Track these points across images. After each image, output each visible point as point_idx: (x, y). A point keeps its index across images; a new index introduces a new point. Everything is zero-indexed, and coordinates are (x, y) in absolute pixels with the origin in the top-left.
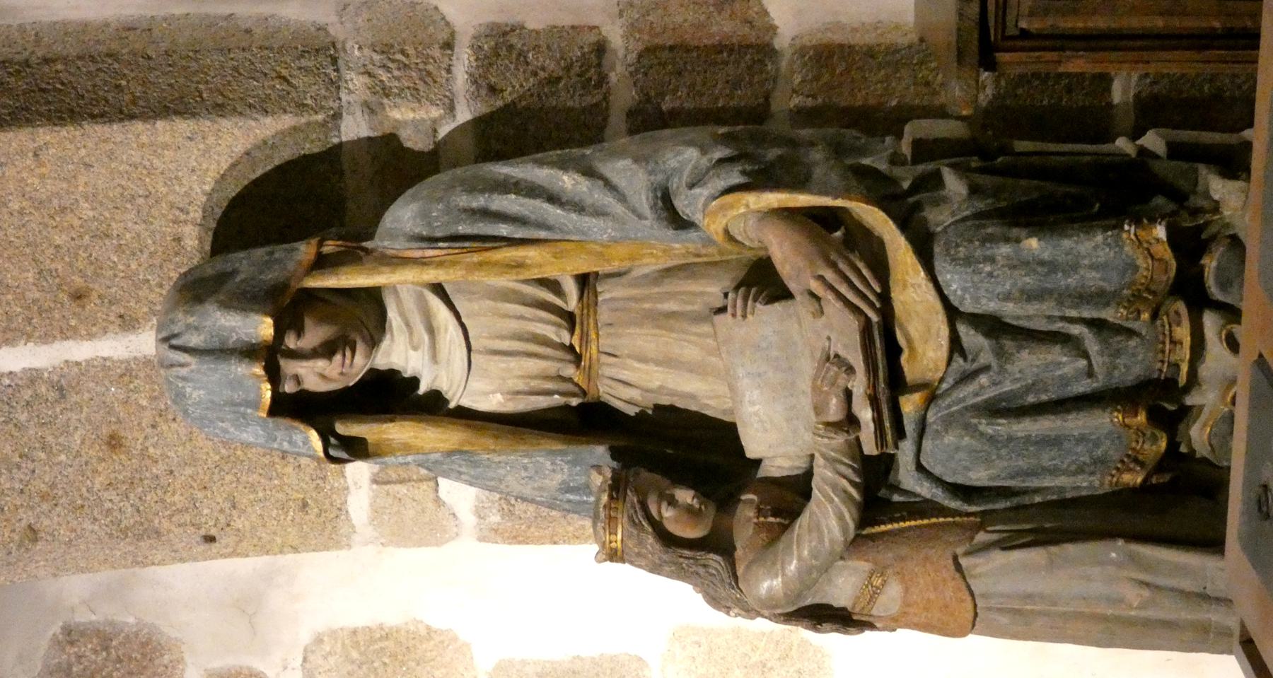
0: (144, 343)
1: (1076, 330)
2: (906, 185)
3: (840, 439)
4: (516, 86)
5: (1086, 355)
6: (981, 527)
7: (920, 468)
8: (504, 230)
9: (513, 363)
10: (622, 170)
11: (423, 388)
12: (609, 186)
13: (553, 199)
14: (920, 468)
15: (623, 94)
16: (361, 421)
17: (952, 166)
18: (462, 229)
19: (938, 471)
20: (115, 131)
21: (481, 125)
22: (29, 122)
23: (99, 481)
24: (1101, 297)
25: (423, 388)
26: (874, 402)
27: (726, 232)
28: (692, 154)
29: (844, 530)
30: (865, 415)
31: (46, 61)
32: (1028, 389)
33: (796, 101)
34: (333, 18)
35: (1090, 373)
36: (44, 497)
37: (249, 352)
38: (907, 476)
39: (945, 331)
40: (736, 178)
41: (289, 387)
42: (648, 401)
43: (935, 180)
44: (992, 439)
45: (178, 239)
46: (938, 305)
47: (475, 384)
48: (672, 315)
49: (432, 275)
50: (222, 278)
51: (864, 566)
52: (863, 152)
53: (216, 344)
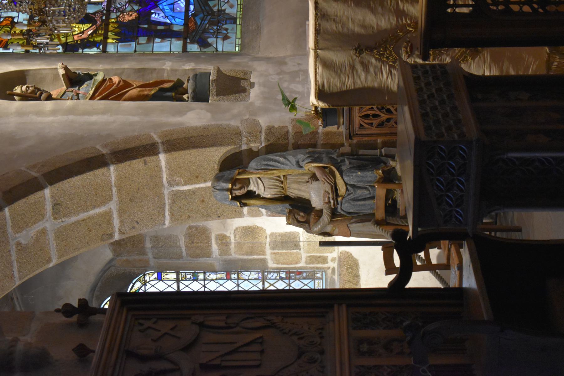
0: (209, 184)
1: (368, 187)
2: (339, 161)
3: (327, 205)
4: (273, 139)
5: (369, 191)
6: (351, 219)
7: (341, 209)
8: (270, 168)
9: (272, 190)
10: (290, 158)
11: (256, 193)
12: (288, 160)
13: (279, 162)
14: (341, 209)
15: (291, 140)
16: (246, 200)
17: (347, 158)
18: (263, 168)
19: (344, 210)
20: (203, 150)
21: (266, 146)
22: (189, 149)
23: (200, 208)
24: (371, 182)
25: (256, 193)
26: (333, 199)
27: (308, 169)
28: (302, 155)
29: (328, 220)
30: (332, 201)
31: (192, 137)
32: (360, 196)
33: (322, 142)
34: (240, 125)
35: (370, 194)
36: (191, 211)
37: (227, 190)
38: (339, 210)
39: (345, 187)
40: (310, 161)
41: (234, 195)
42: (296, 196)
43: (343, 161)
44: (353, 205)
45: (214, 167)
46: (344, 183)
47: (265, 193)
48: (300, 182)
49: (258, 176)
50: (222, 177)
51: (332, 226)
52: (332, 154)
53: (222, 188)
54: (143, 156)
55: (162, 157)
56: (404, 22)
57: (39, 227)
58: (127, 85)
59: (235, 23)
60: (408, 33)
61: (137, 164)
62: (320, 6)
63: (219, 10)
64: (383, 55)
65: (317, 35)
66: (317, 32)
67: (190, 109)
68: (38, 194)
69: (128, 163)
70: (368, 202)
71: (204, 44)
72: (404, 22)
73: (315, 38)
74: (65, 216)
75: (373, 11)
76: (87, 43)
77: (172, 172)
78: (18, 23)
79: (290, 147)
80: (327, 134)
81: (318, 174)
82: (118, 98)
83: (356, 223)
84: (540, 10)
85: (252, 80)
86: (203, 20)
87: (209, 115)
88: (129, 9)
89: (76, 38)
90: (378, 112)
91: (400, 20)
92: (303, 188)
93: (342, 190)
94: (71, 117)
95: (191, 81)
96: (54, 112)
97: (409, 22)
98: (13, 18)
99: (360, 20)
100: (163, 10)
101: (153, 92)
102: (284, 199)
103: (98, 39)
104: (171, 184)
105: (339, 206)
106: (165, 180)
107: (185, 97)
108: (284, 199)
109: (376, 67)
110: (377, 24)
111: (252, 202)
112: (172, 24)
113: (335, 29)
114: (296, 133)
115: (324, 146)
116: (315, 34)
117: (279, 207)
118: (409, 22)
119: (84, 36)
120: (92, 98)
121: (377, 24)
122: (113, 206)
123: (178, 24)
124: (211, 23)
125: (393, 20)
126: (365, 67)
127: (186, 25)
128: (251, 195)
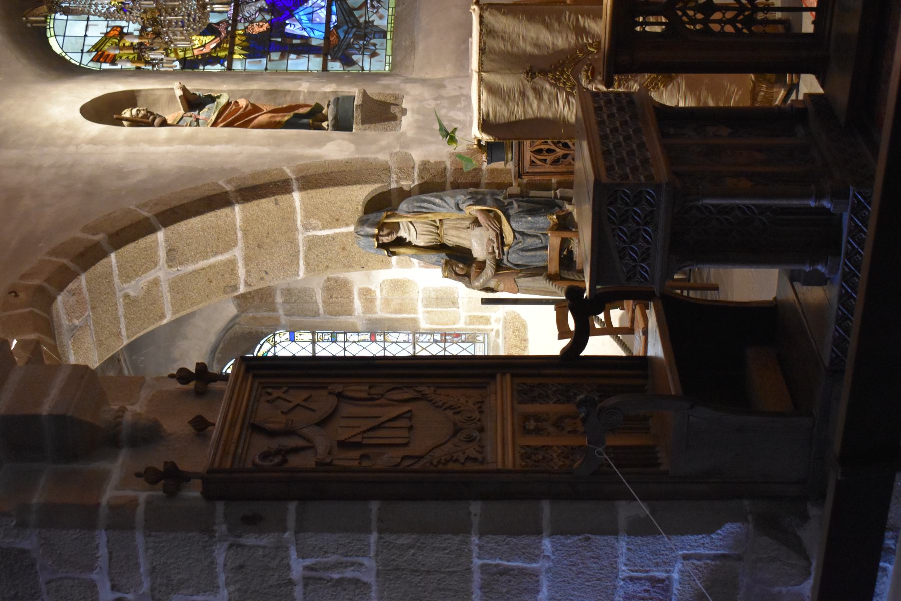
1: (539, 235)
2: (506, 204)
3: (491, 256)
4: (427, 177)
5: (541, 239)
6: (519, 273)
7: (508, 261)
8: (424, 210)
9: (426, 237)
10: (448, 199)
11: (407, 241)
12: (446, 202)
13: (434, 204)
14: (508, 261)
15: (450, 178)
17: (515, 200)
18: (416, 210)
19: (511, 262)
20: (345, 188)
21: (420, 185)
22: (328, 187)
23: (341, 257)
24: (543, 229)
25: (407, 241)
26: (498, 249)
27: (469, 213)
28: (462, 197)
29: (492, 274)
30: (496, 251)
31: (331, 173)
32: (530, 246)
33: (486, 181)
34: (389, 159)
35: (542, 243)
36: (330, 260)
37: (373, 236)
38: (505, 262)
39: (512, 235)
40: (471, 203)
41: (381, 242)
42: (455, 244)
43: (511, 204)
44: (522, 256)
45: (357, 208)
46: (511, 230)
47: (418, 240)
48: (459, 228)
49: (410, 220)
50: (368, 220)
51: (496, 280)
52: (498, 195)
53: (366, 234)
54: (274, 194)
55: (297, 196)
56: (585, 41)
57: (150, 276)
58: (256, 109)
59: (385, 37)
60: (589, 54)
61: (266, 204)
62: (485, 20)
63: (366, 21)
64: (559, 79)
65: (482, 54)
66: (482, 51)
67: (332, 140)
68: (150, 238)
69: (256, 202)
70: (538, 253)
71: (348, 61)
72: (585, 41)
73: (479, 59)
74: (181, 264)
75: (548, 27)
76: (209, 59)
77: (308, 214)
78: (127, 34)
79: (448, 185)
80: (492, 171)
81: (481, 219)
82: (245, 125)
83: (524, 277)
84: (745, 31)
85: (404, 106)
86: (347, 32)
87: (352, 147)
88: (259, 18)
89: (196, 52)
90: (553, 147)
91: (580, 39)
92: (462, 235)
93: (509, 238)
94: (189, 147)
95: (332, 106)
96: (169, 141)
97: (590, 41)
98: (122, 28)
99: (532, 38)
100: (300, 21)
101: (286, 118)
102: (440, 247)
103: (222, 54)
104: (306, 229)
105: (505, 257)
106: (299, 223)
107: (325, 124)
108: (440, 247)
109: (550, 94)
110: (553, 44)
111: (402, 250)
112: (310, 37)
113: (503, 47)
114: (455, 169)
115: (488, 185)
116: (479, 53)
117: (434, 257)
118: (590, 41)
119: (206, 50)
120: (215, 124)
121: (553, 44)
122: (238, 253)
123: (318, 37)
124: (357, 37)
125: (572, 39)
126: (538, 93)
127: (327, 38)
128: (401, 242)
